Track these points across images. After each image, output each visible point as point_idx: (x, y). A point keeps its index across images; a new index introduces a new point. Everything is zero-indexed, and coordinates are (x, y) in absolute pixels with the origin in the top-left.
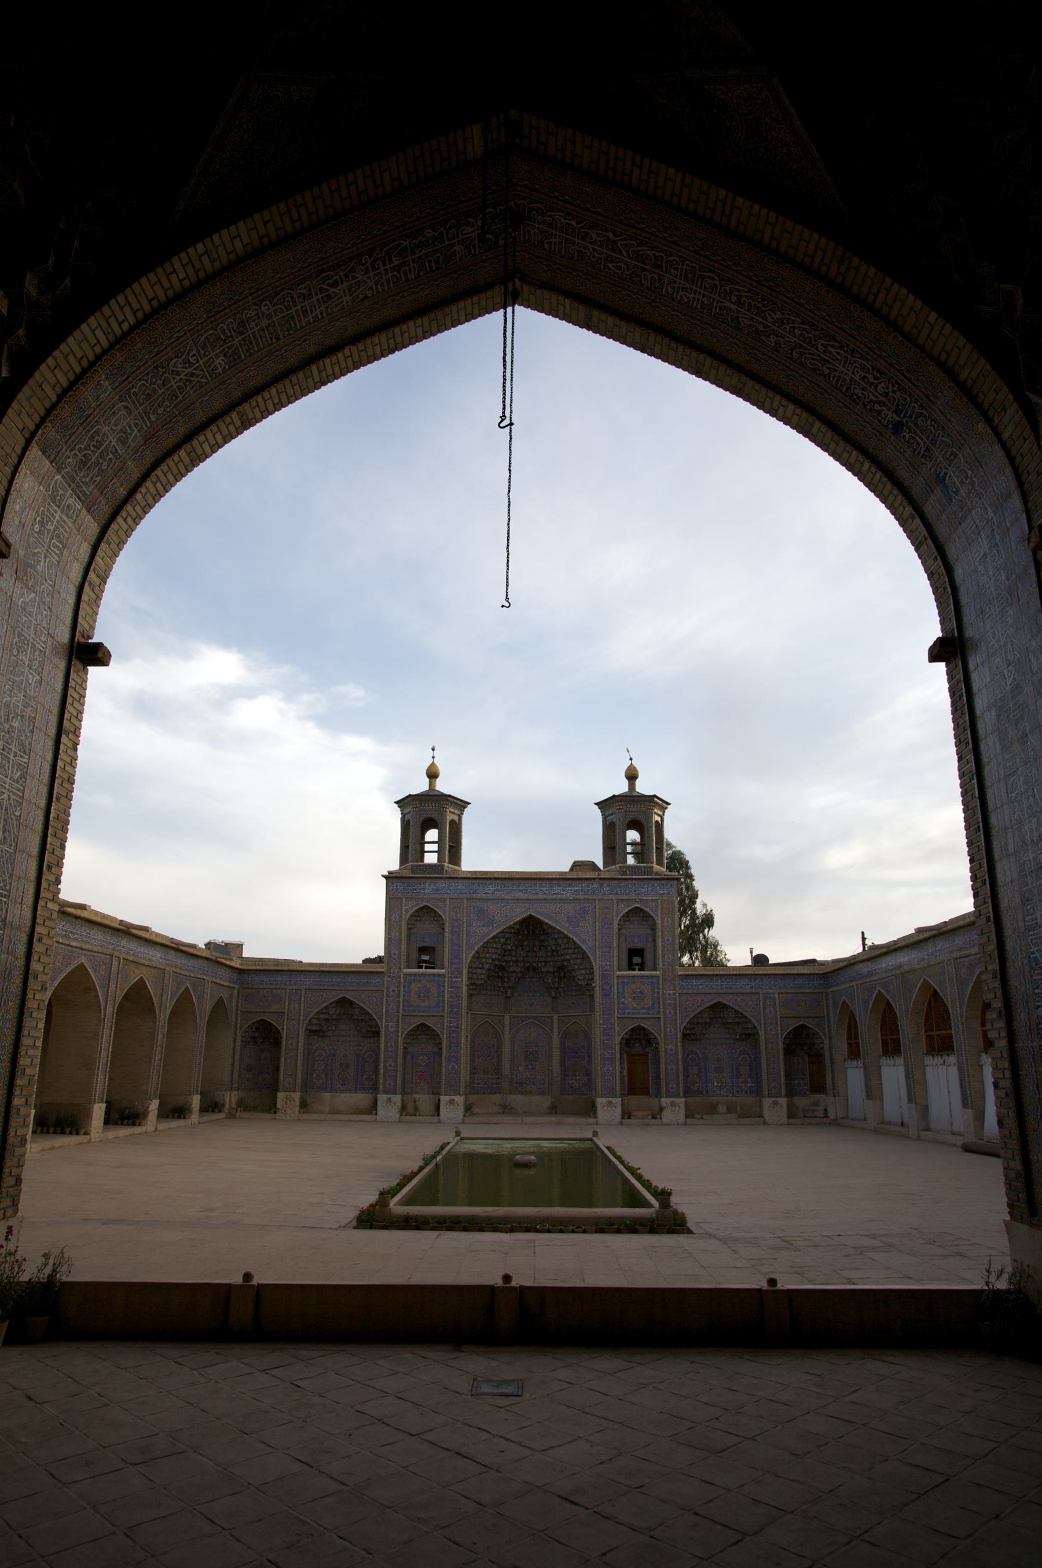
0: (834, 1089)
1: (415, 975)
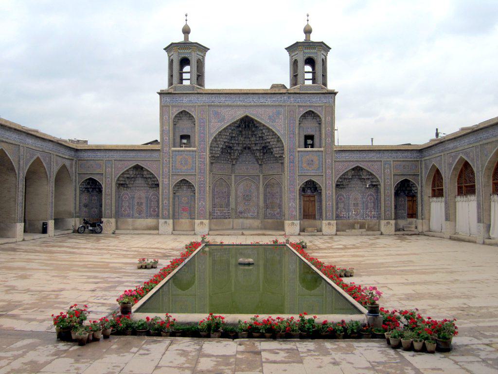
0: (422, 215)
1: (178, 151)
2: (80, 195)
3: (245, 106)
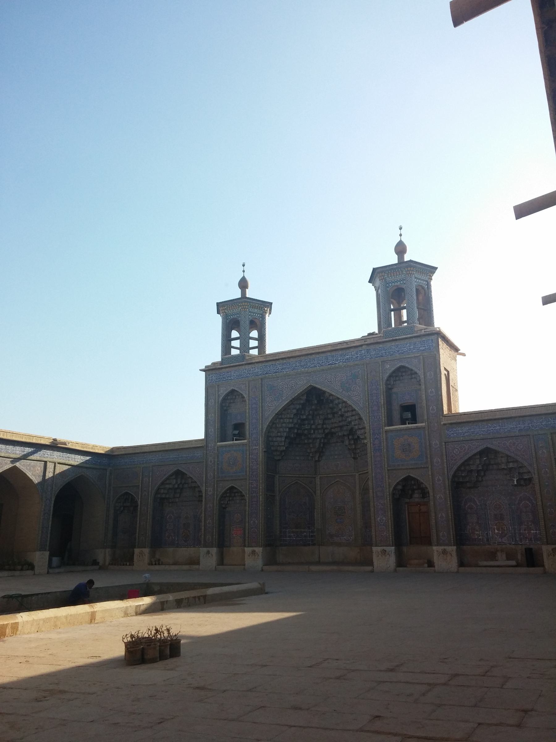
3: (308, 373)
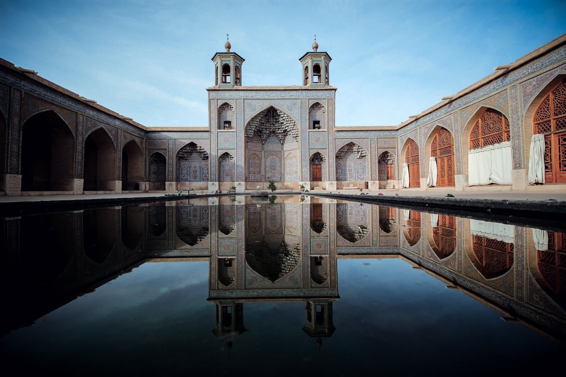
2: (149, 165)
